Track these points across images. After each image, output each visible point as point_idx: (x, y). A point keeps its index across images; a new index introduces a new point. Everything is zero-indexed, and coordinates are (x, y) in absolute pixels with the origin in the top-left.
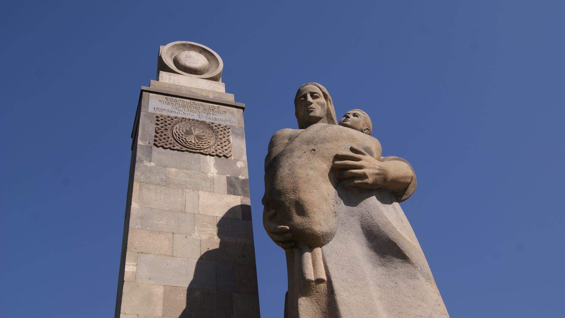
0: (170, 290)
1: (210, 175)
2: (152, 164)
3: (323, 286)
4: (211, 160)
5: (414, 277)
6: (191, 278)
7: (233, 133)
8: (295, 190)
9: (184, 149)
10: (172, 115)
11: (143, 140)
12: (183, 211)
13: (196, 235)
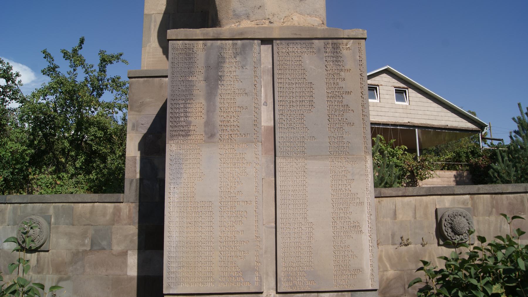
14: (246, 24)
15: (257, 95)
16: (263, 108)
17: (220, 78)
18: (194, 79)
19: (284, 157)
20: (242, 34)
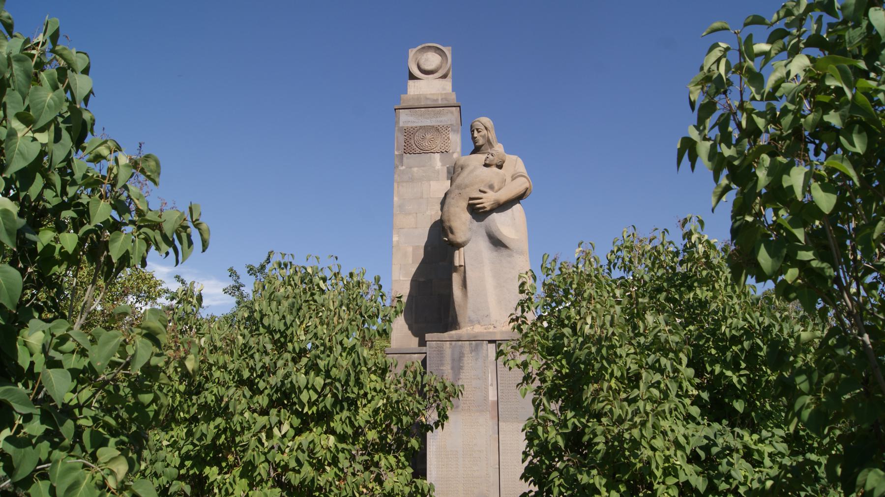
0: (415, 248)
1: (437, 168)
2: (404, 167)
3: (462, 268)
4: (437, 156)
5: (510, 256)
6: (426, 239)
7: (452, 130)
8: (449, 221)
9: (422, 151)
10: (414, 125)
11: (398, 150)
12: (422, 198)
13: (428, 213)
14: (478, 329)
15: (486, 379)
16: (490, 388)
17: (461, 368)
18: (444, 368)
19: (504, 421)
20: (475, 337)
